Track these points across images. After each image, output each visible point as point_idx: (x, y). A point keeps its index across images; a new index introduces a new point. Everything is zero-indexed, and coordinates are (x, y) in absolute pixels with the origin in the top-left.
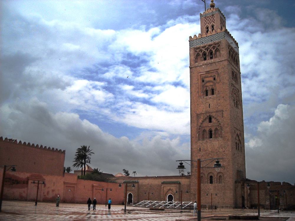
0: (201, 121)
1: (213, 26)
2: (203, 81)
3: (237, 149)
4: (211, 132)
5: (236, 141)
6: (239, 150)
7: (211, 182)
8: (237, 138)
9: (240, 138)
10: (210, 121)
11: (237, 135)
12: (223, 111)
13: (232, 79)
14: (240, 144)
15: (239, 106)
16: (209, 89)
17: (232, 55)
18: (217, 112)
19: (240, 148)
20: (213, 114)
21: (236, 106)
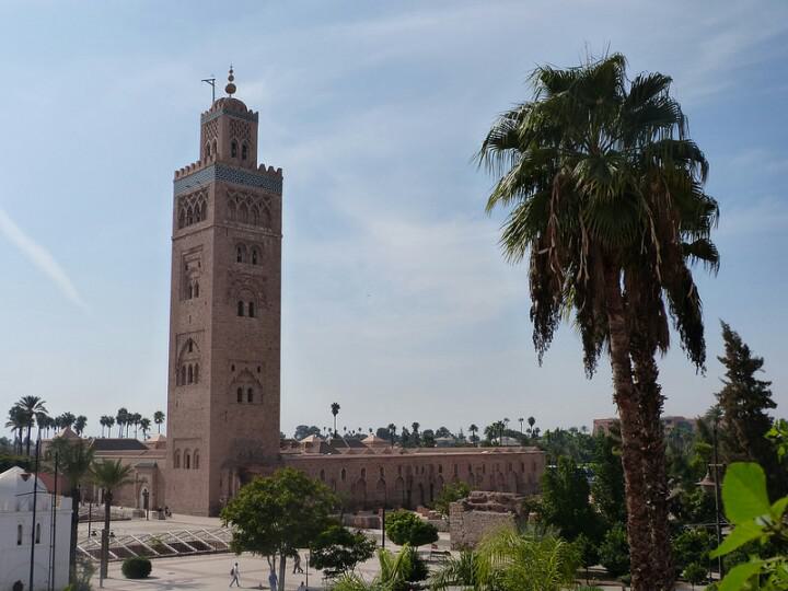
0: (179, 350)
1: (215, 144)
2: (187, 268)
3: (240, 400)
4: (190, 368)
5: (241, 385)
6: (250, 400)
7: (188, 467)
8: (246, 379)
9: (257, 376)
10: (191, 350)
11: (247, 372)
12: (204, 331)
13: (239, 260)
14: (256, 391)
15: (260, 312)
16: (193, 284)
17: (243, 207)
18: (197, 332)
19: (255, 399)
20: (193, 336)
21: (246, 312)
